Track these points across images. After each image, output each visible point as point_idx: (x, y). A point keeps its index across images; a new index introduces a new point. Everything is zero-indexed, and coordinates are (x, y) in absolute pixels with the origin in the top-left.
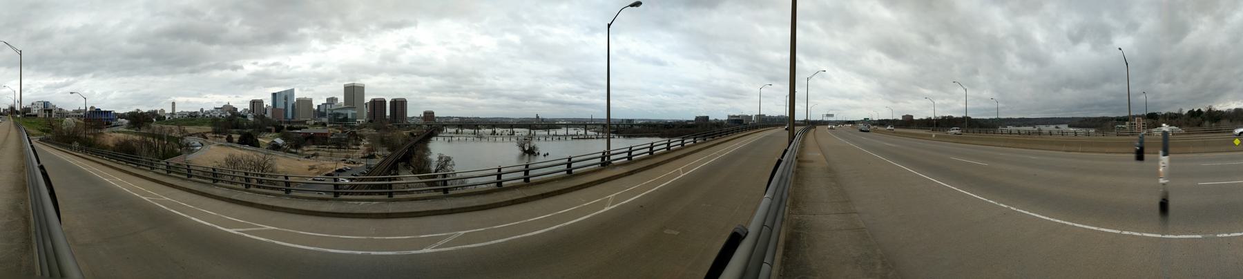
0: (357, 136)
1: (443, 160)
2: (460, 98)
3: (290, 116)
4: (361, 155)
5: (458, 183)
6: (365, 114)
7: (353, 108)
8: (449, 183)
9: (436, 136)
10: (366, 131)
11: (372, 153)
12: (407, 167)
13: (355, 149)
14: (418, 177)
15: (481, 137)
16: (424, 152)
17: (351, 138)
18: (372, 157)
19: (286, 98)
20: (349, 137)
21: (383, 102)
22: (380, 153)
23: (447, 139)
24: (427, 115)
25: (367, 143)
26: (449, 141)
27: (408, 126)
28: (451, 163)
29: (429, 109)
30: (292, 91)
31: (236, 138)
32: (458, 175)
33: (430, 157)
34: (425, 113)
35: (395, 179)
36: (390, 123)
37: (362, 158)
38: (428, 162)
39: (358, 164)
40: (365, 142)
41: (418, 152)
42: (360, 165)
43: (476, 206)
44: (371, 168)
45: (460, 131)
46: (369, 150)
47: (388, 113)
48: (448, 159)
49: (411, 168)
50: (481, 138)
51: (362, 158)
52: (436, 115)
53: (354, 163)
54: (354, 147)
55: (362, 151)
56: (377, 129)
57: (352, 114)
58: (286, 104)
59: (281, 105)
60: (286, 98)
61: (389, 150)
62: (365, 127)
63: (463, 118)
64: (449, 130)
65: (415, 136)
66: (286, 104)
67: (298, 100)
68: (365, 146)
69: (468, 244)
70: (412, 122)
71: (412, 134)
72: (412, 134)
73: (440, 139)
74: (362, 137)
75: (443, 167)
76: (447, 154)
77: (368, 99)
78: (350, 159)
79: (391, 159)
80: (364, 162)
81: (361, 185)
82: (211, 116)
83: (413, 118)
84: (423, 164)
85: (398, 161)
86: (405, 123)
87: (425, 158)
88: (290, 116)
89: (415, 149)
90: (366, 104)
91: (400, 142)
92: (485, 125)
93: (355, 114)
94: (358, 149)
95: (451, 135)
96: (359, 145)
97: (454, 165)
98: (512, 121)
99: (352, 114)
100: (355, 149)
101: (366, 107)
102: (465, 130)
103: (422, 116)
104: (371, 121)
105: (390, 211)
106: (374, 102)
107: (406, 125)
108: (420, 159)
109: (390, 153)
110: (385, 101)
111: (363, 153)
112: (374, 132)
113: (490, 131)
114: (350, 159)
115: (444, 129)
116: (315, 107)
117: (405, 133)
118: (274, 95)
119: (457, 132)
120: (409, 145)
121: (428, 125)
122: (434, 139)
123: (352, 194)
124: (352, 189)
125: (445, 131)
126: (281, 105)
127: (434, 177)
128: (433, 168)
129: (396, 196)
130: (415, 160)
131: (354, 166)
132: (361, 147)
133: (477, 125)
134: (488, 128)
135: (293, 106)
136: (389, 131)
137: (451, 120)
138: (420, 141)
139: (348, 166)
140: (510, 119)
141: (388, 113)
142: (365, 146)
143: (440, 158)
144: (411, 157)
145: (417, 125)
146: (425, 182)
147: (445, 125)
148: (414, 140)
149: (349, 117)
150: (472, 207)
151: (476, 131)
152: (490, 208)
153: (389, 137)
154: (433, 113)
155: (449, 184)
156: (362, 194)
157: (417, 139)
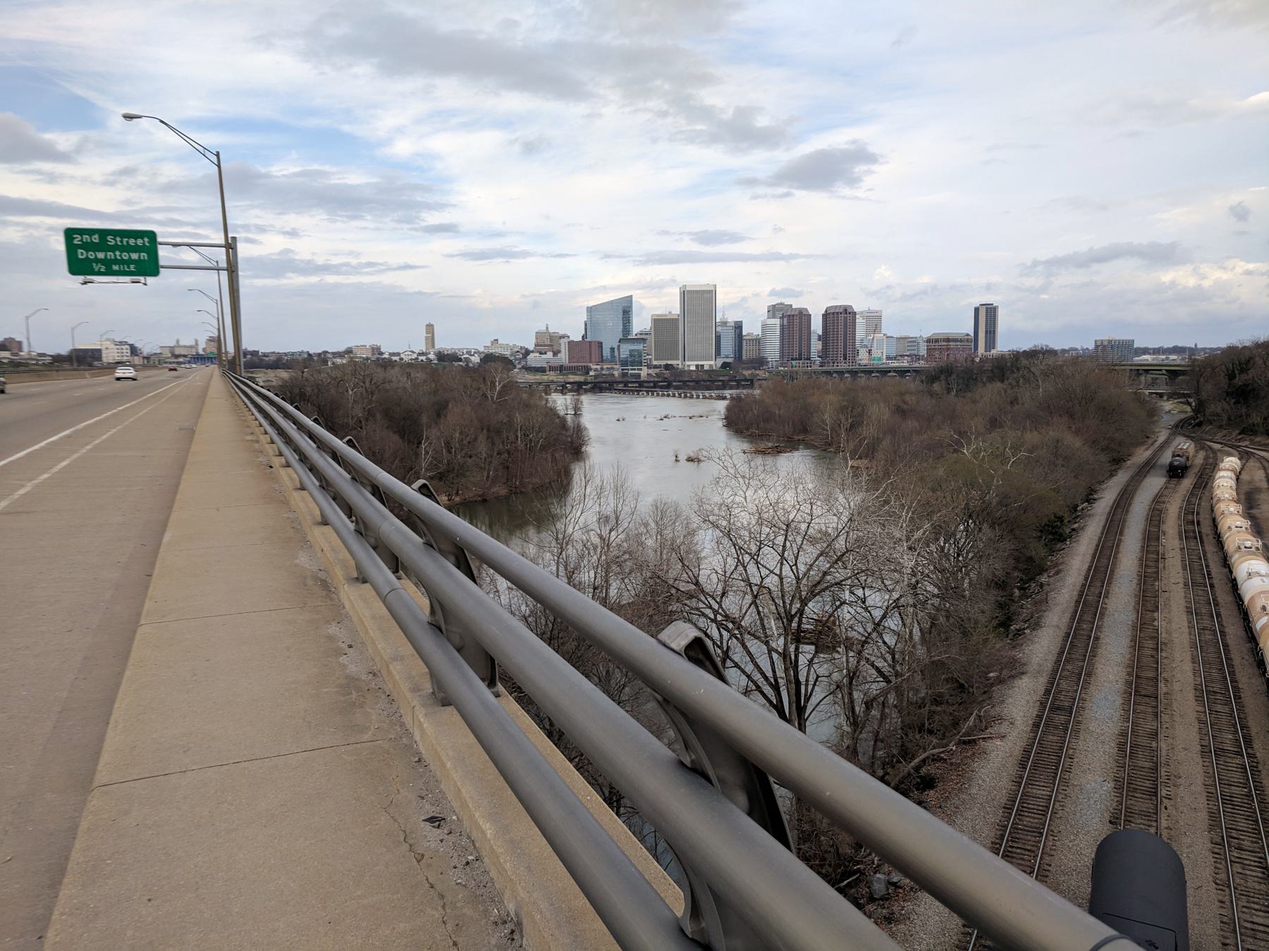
47: (816, 346)
99: (631, 351)
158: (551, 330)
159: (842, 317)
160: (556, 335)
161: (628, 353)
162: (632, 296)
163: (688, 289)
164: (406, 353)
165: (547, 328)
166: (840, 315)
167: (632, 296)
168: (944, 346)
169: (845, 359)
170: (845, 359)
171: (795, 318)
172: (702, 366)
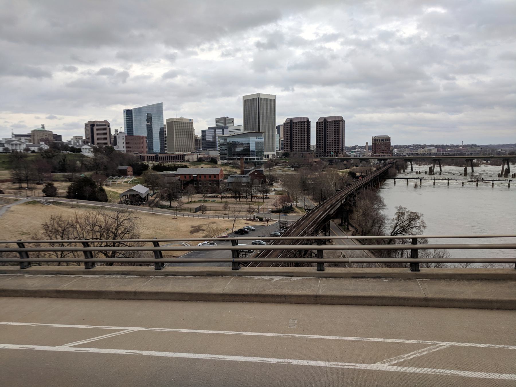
0: (264, 177)
1: (406, 217)
2: (413, 115)
3: (157, 148)
4: (271, 208)
5: (431, 254)
6: (277, 144)
7: (258, 134)
8: (420, 253)
9: (394, 177)
10: (278, 171)
11: (288, 204)
12: (344, 226)
13: (263, 198)
14: (358, 240)
15: (478, 180)
16: (373, 204)
17: (256, 181)
18: (289, 210)
19: (149, 119)
20: (252, 180)
21: (305, 124)
22: (300, 204)
23: (412, 183)
24: (379, 143)
25: (281, 189)
26: (416, 186)
27: (346, 162)
28: (418, 223)
29: (381, 133)
30: (159, 107)
31: (63, 188)
32: (431, 242)
33: (382, 212)
34: (375, 140)
35: (324, 242)
36: (317, 157)
37: (273, 212)
38: (379, 221)
39: (267, 221)
40: (278, 187)
41: (363, 203)
42: (270, 223)
43: (473, 301)
44: (287, 228)
45: (437, 169)
46: (284, 200)
47: (313, 141)
48: (414, 217)
49: (351, 229)
50: (478, 182)
51: (273, 212)
52: (393, 143)
53: (261, 220)
54: (260, 195)
55: (273, 201)
56: (296, 167)
57: (257, 143)
58: (150, 128)
59: (140, 130)
60: (149, 119)
61: (315, 200)
62: (277, 164)
63: (443, 147)
64: (416, 168)
65: (358, 178)
66: (150, 128)
67: (170, 123)
68: (278, 193)
69: (459, 369)
70: (352, 155)
71: (352, 175)
72: (352, 175)
73: (399, 182)
74: (273, 180)
75: (404, 230)
76: (411, 208)
77: (280, 121)
78: (255, 214)
79: (318, 214)
80: (276, 219)
81: (275, 250)
82: (6, 150)
83: (354, 148)
84: (370, 223)
85: (328, 218)
86: (340, 156)
87: (373, 214)
88: (157, 148)
89: (357, 199)
90: (278, 128)
91: (333, 187)
92: (486, 159)
93: (260, 143)
94: (267, 198)
95: (421, 176)
96: (267, 192)
97: (424, 227)
98: (426, 150)
99: (257, 143)
100: (263, 198)
101: (279, 132)
102: (447, 168)
103: (370, 144)
104: (286, 155)
105: (320, 293)
106: (290, 124)
107: (342, 160)
108: (366, 215)
109: (316, 204)
110: (308, 122)
111: (275, 205)
112: (291, 171)
113: (498, 169)
114: (255, 214)
115: (407, 167)
116: (198, 134)
117: (341, 172)
118: (129, 113)
119: (431, 172)
120: (347, 191)
121: (380, 160)
122: (390, 182)
123: (262, 264)
124: (263, 256)
125: (409, 169)
126: (140, 130)
127: (391, 241)
128: (387, 232)
129: (329, 270)
130: (356, 215)
131: (261, 224)
132: (272, 195)
133: (471, 159)
134: (491, 164)
135: (162, 132)
136: (316, 170)
137: (421, 151)
138: (365, 186)
139: (252, 225)
140: (424, 146)
141: (313, 141)
142: (278, 193)
143: (400, 214)
144: (351, 211)
145: (362, 160)
146: (370, 250)
147: (410, 160)
148: (355, 185)
149: (253, 148)
150: (465, 301)
151: (469, 169)
152: (498, 309)
153: (314, 179)
154: (389, 139)
155: (422, 256)
156: (277, 264)
157: (362, 182)
158: (47, 129)
159: (341, 123)
160: (49, 133)
161: (255, 145)
162: (161, 104)
163: (261, 97)
164: (14, 143)
165: (43, 127)
166: (340, 123)
167: (161, 104)
168: (387, 143)
169: (342, 151)
170: (342, 151)
171: (305, 124)
172: (268, 155)
